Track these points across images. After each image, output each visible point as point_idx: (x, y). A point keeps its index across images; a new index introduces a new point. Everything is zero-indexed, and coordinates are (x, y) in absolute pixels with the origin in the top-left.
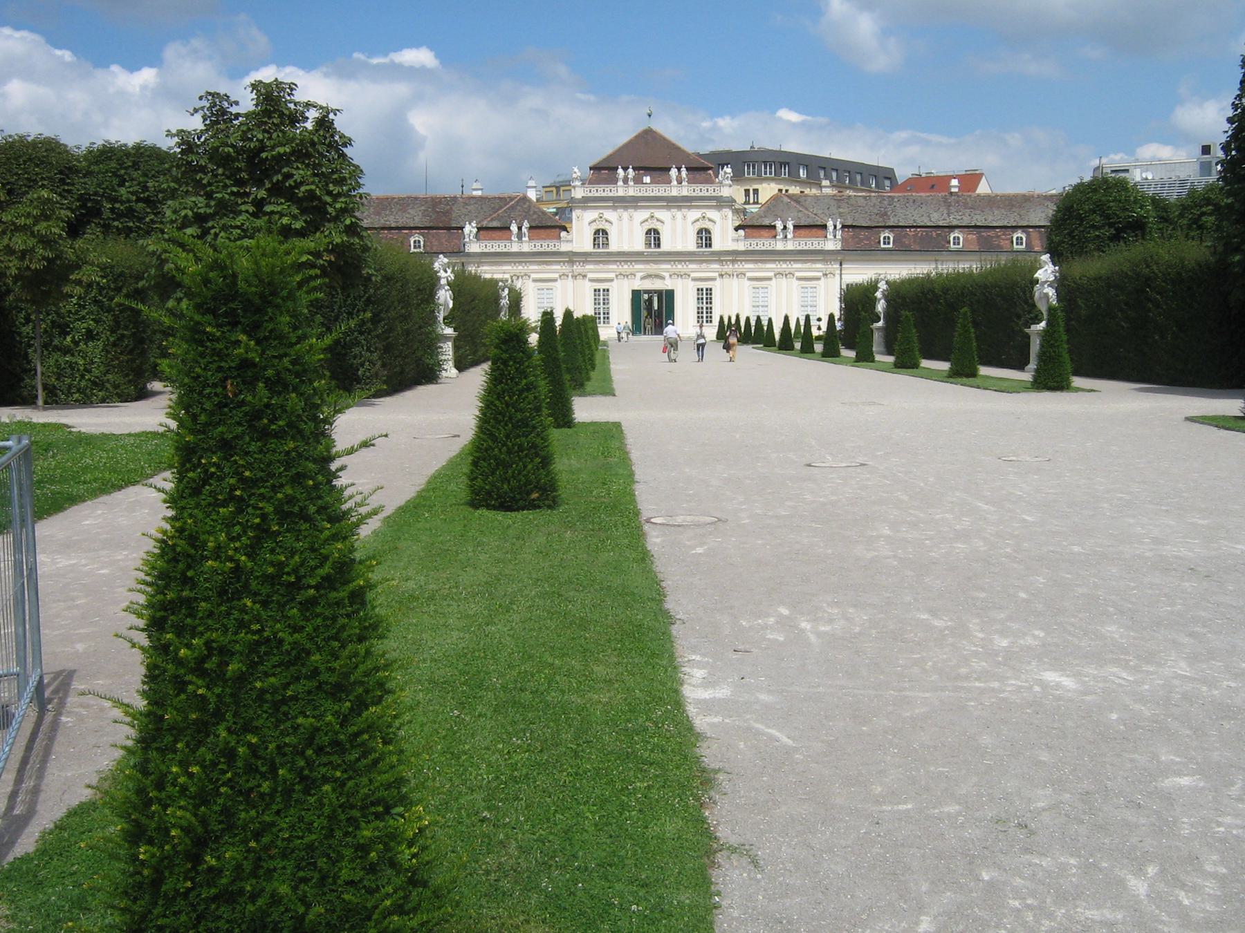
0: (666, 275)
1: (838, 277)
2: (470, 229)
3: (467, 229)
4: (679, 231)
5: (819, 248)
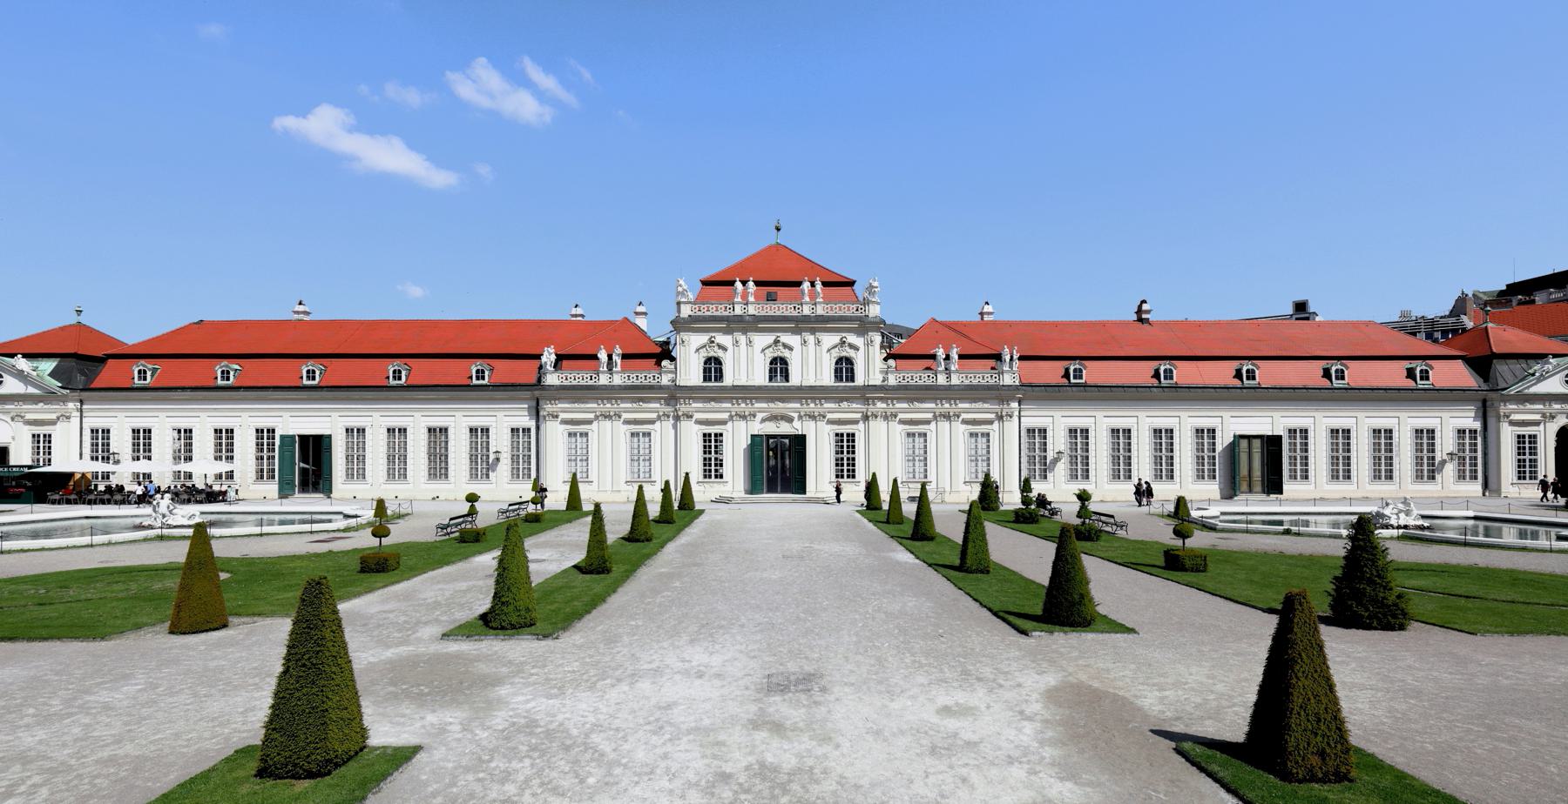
0: (795, 415)
1: (1016, 419)
2: (548, 357)
3: (544, 359)
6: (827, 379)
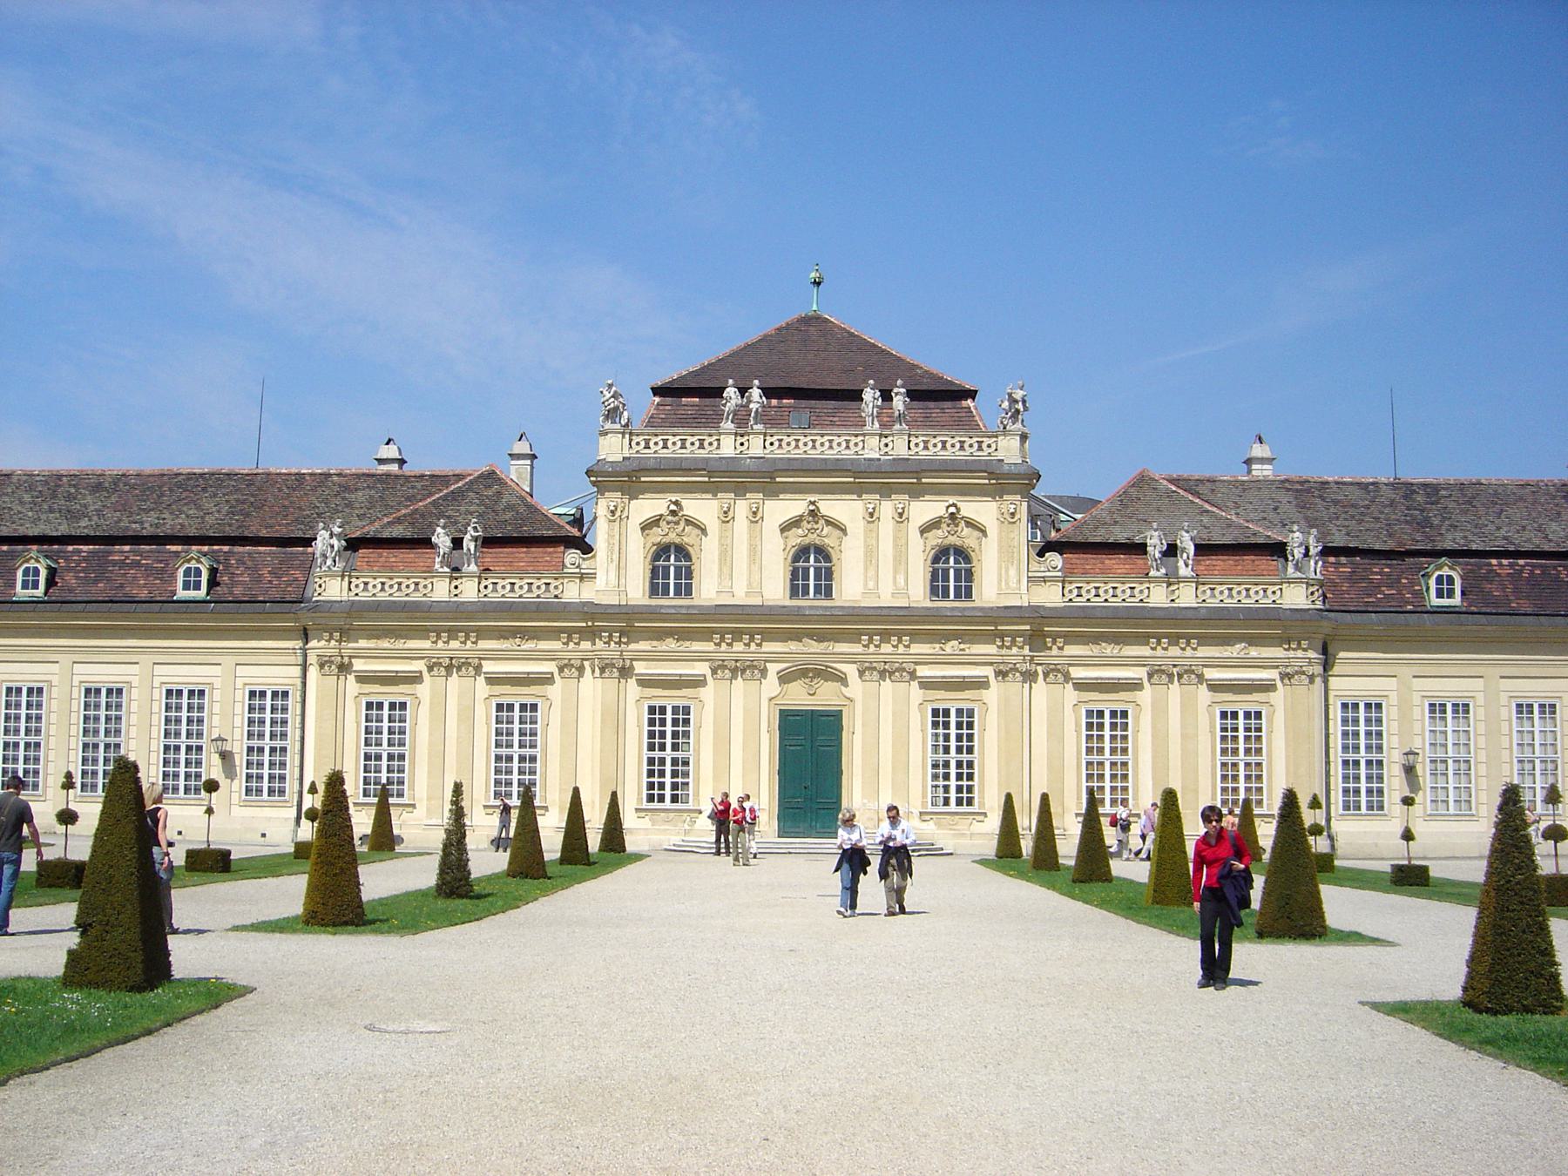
0: (851, 670)
3: (320, 545)
4: (881, 557)
5: (1266, 602)
6: (917, 593)
